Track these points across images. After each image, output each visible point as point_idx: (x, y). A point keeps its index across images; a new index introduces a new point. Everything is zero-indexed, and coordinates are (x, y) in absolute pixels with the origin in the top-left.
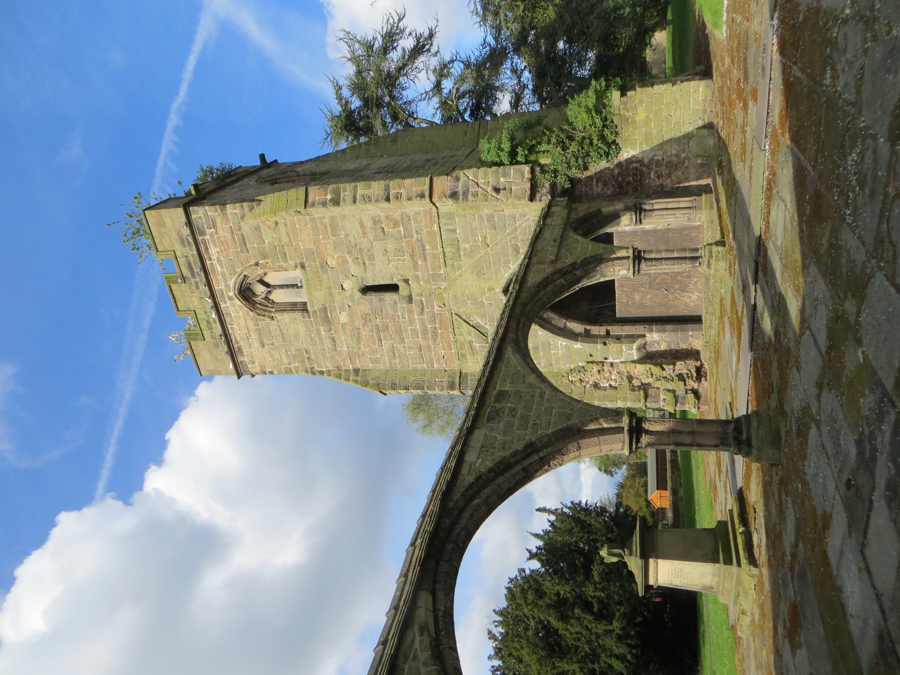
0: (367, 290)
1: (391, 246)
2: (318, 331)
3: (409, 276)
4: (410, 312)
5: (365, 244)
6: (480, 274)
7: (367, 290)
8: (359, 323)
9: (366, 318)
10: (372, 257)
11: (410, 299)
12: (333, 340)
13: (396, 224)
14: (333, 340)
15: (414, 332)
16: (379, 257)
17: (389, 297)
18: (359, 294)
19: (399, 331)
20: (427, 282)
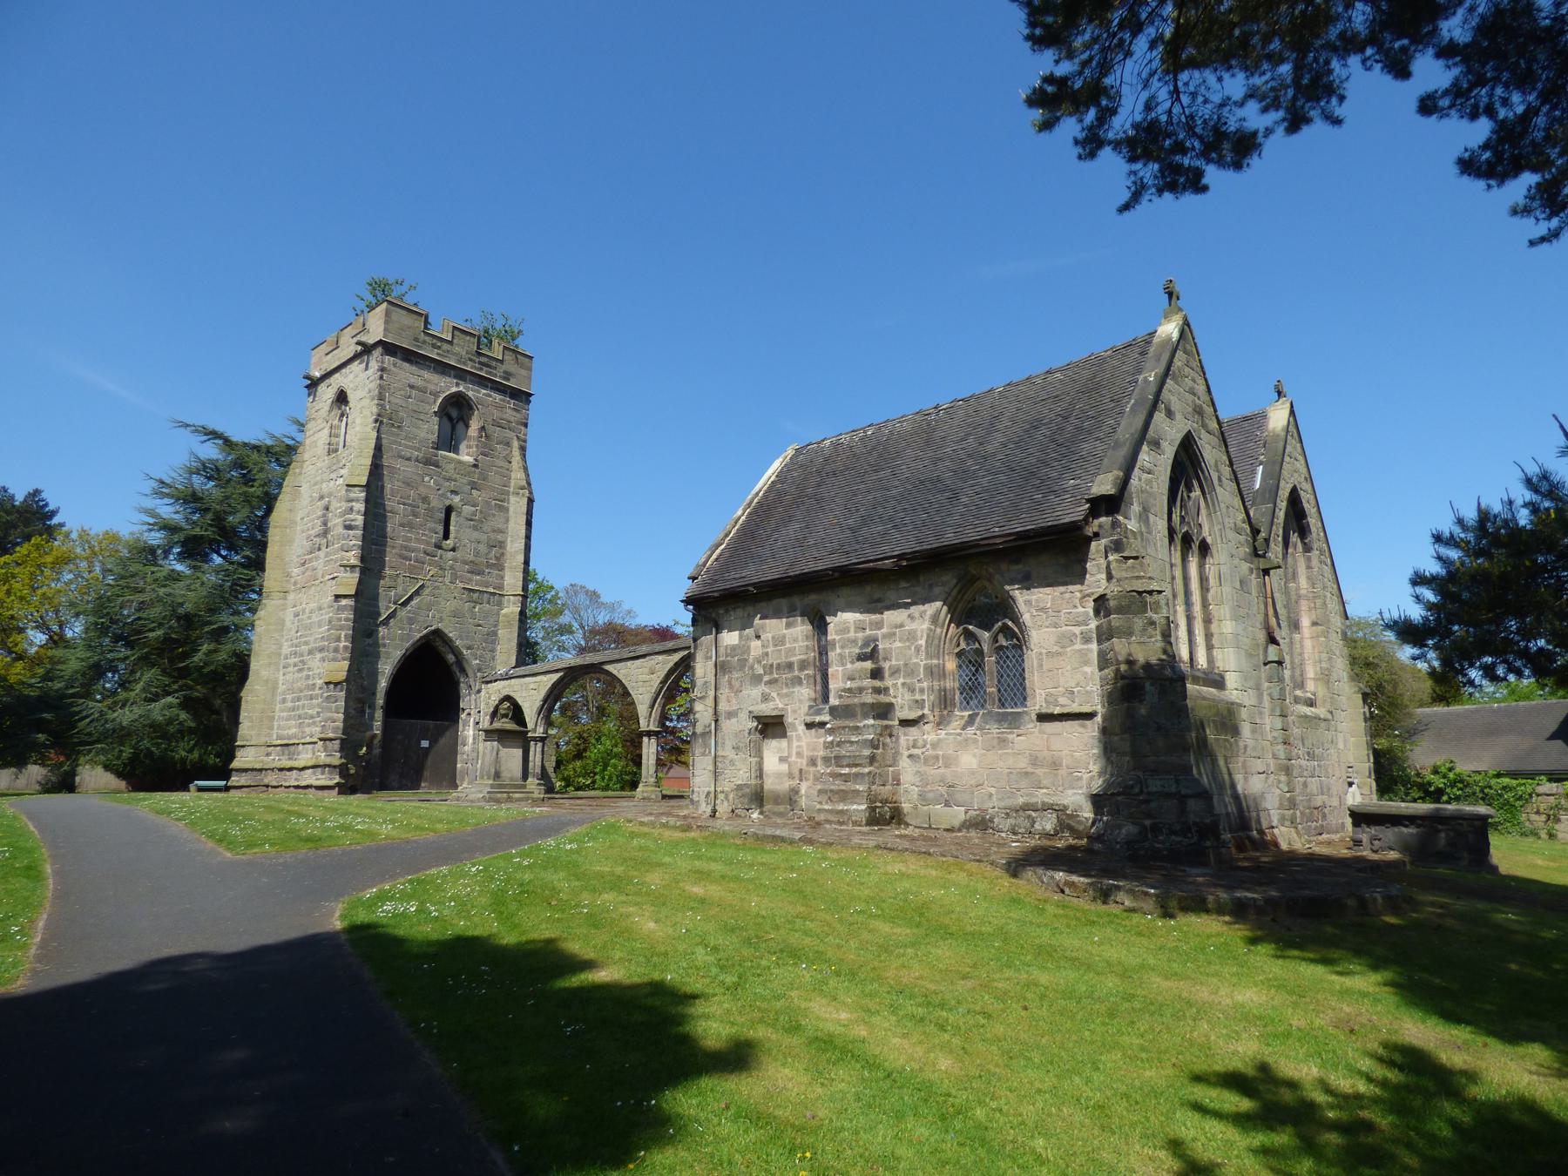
0: (449, 510)
1: (483, 548)
2: (418, 450)
3: (458, 554)
4: (428, 543)
5: (486, 528)
6: (456, 614)
7: (449, 510)
8: (422, 490)
9: (425, 499)
10: (475, 528)
11: (439, 547)
12: (409, 459)
13: (498, 559)
14: (409, 459)
15: (410, 540)
16: (476, 535)
17: (440, 528)
18: (448, 503)
19: (411, 526)
20: (452, 568)
